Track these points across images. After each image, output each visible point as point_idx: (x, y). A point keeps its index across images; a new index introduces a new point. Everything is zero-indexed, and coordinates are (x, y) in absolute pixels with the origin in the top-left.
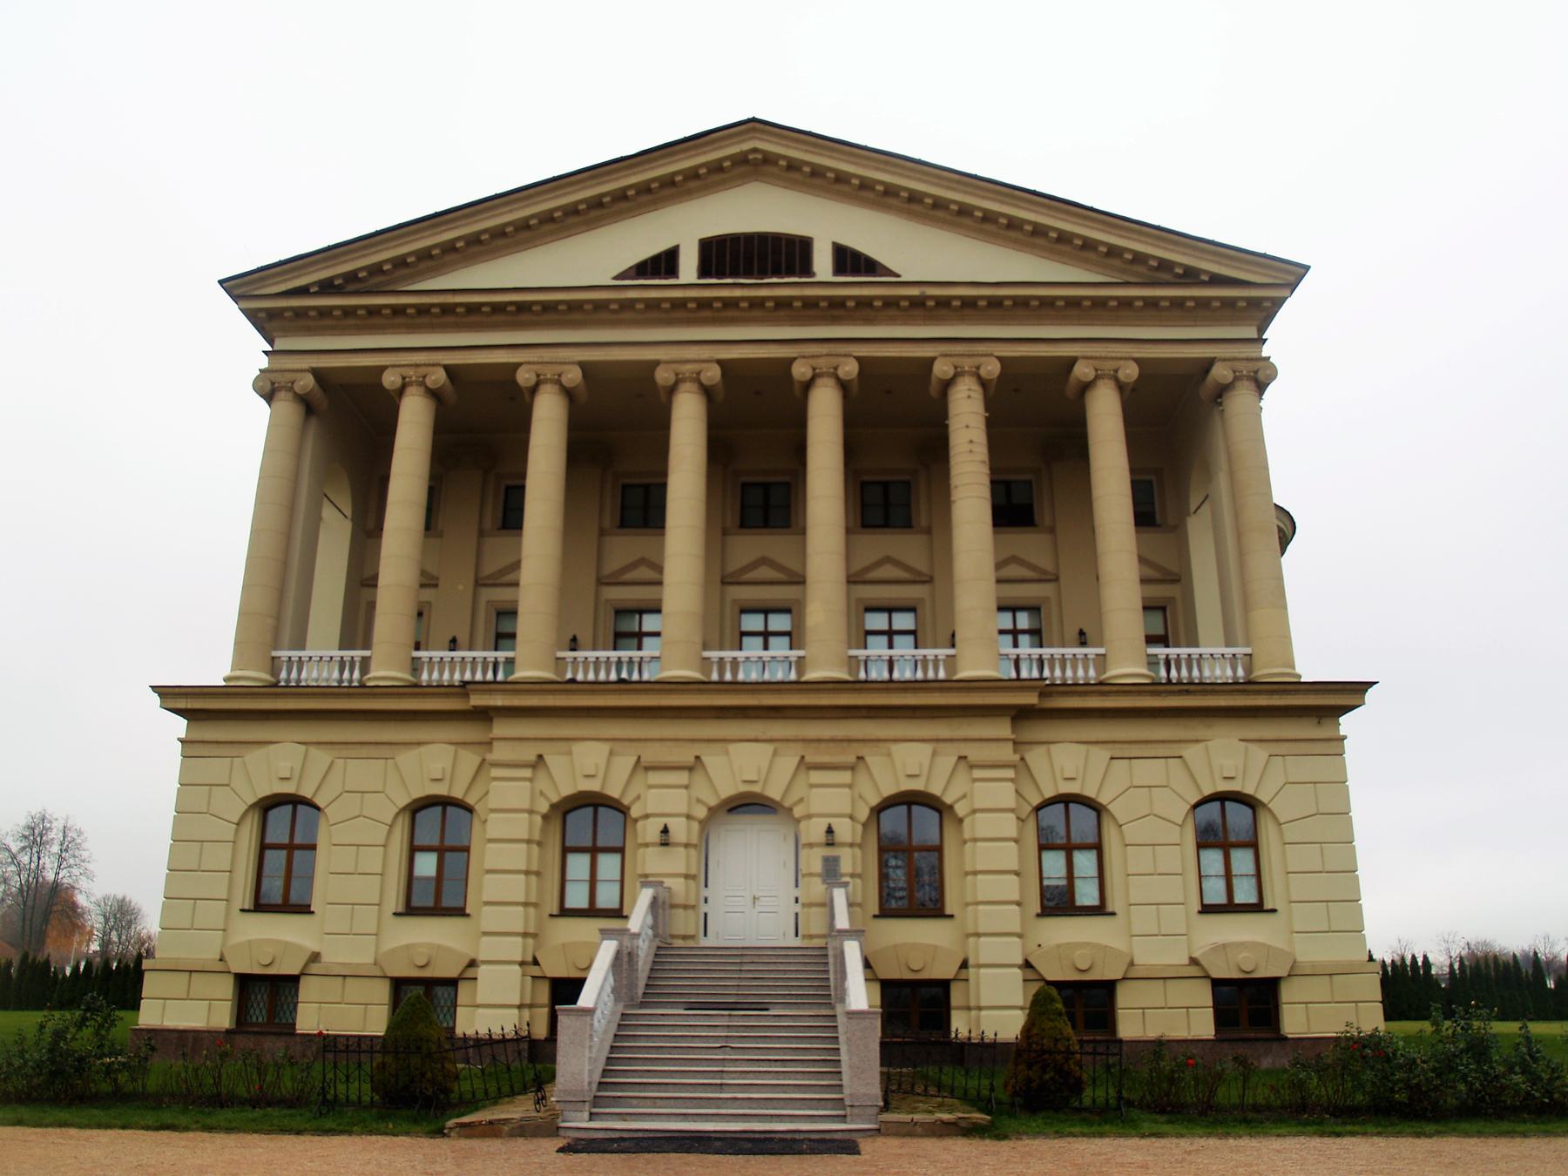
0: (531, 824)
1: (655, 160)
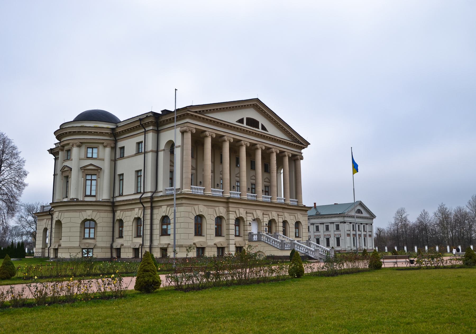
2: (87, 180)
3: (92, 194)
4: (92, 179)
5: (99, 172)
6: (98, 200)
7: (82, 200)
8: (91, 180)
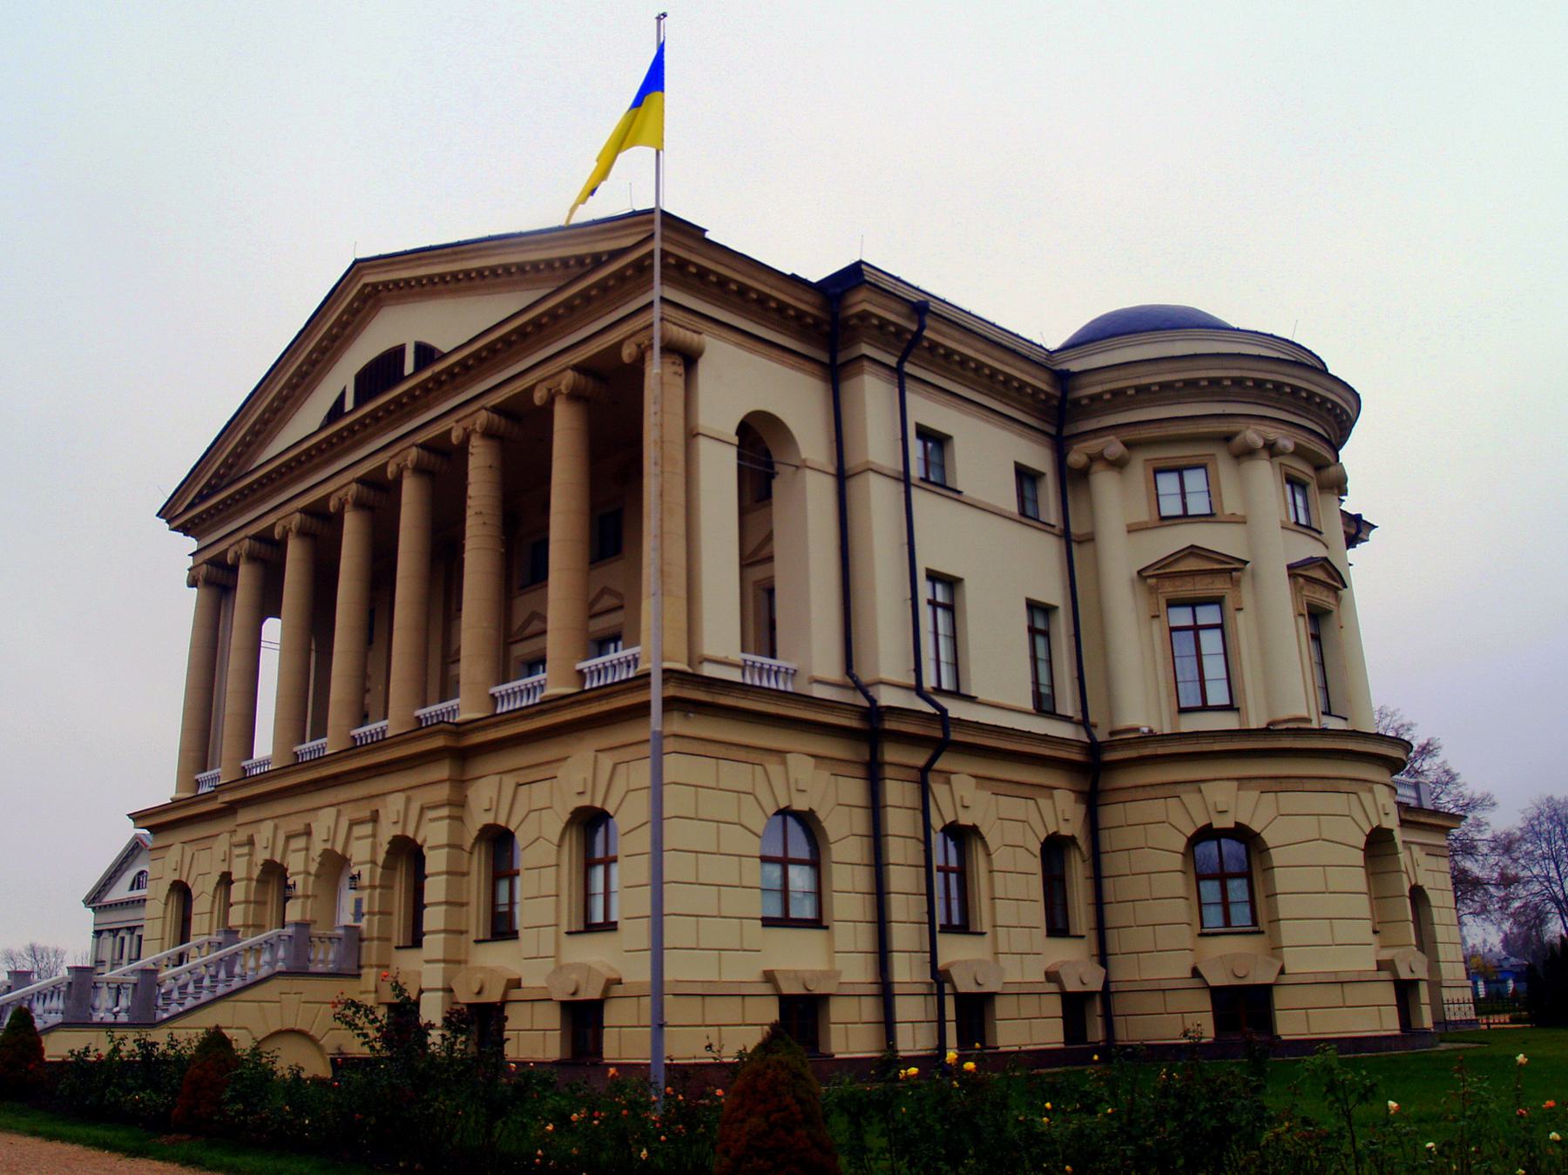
0: (248, 887)
1: (318, 323)
2: (1173, 629)
3: (1211, 702)
4: (1199, 623)
5: (1236, 583)
6: (1253, 726)
7: (1167, 731)
8: (1196, 629)
